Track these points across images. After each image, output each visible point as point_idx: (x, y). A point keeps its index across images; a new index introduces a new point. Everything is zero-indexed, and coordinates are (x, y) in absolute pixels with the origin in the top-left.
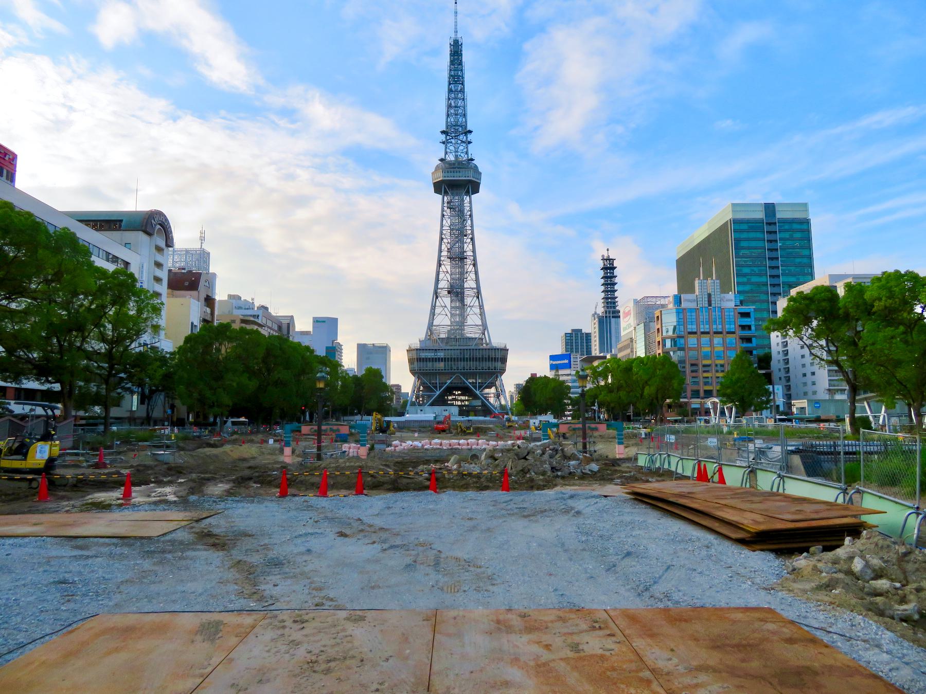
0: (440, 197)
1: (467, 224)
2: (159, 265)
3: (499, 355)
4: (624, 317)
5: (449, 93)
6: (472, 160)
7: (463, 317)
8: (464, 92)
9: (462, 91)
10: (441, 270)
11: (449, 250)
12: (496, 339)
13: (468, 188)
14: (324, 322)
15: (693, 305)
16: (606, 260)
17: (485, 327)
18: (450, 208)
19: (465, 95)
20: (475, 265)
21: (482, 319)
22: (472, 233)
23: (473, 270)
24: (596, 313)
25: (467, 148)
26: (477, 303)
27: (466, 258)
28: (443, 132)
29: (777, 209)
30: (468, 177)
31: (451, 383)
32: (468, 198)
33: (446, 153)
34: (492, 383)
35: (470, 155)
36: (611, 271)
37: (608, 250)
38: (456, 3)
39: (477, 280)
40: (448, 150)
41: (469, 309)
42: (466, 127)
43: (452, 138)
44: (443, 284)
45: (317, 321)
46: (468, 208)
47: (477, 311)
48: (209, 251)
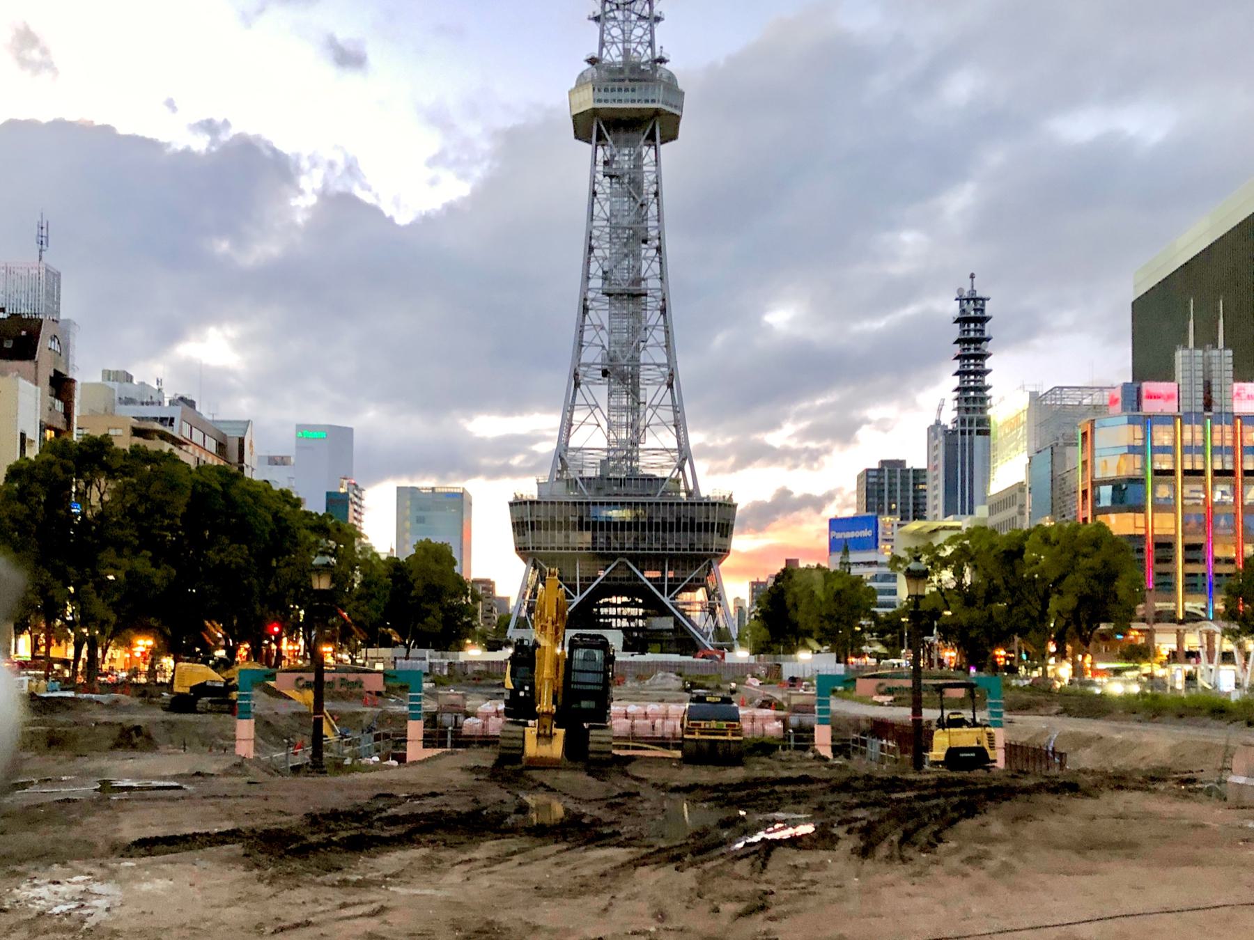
0: (587, 148)
1: (649, 215)
3: (715, 517)
10: (587, 321)
11: (606, 276)
16: (968, 300)
18: (611, 177)
20: (663, 311)
21: (678, 436)
23: (661, 322)
24: (938, 423)
25: (652, 32)
27: (646, 295)
30: (653, 101)
31: (607, 578)
32: (652, 151)
33: (602, 44)
34: (698, 580)
36: (979, 326)
37: (972, 276)
40: (607, 38)
41: (649, 412)
44: (592, 355)
46: (652, 177)
47: (668, 415)
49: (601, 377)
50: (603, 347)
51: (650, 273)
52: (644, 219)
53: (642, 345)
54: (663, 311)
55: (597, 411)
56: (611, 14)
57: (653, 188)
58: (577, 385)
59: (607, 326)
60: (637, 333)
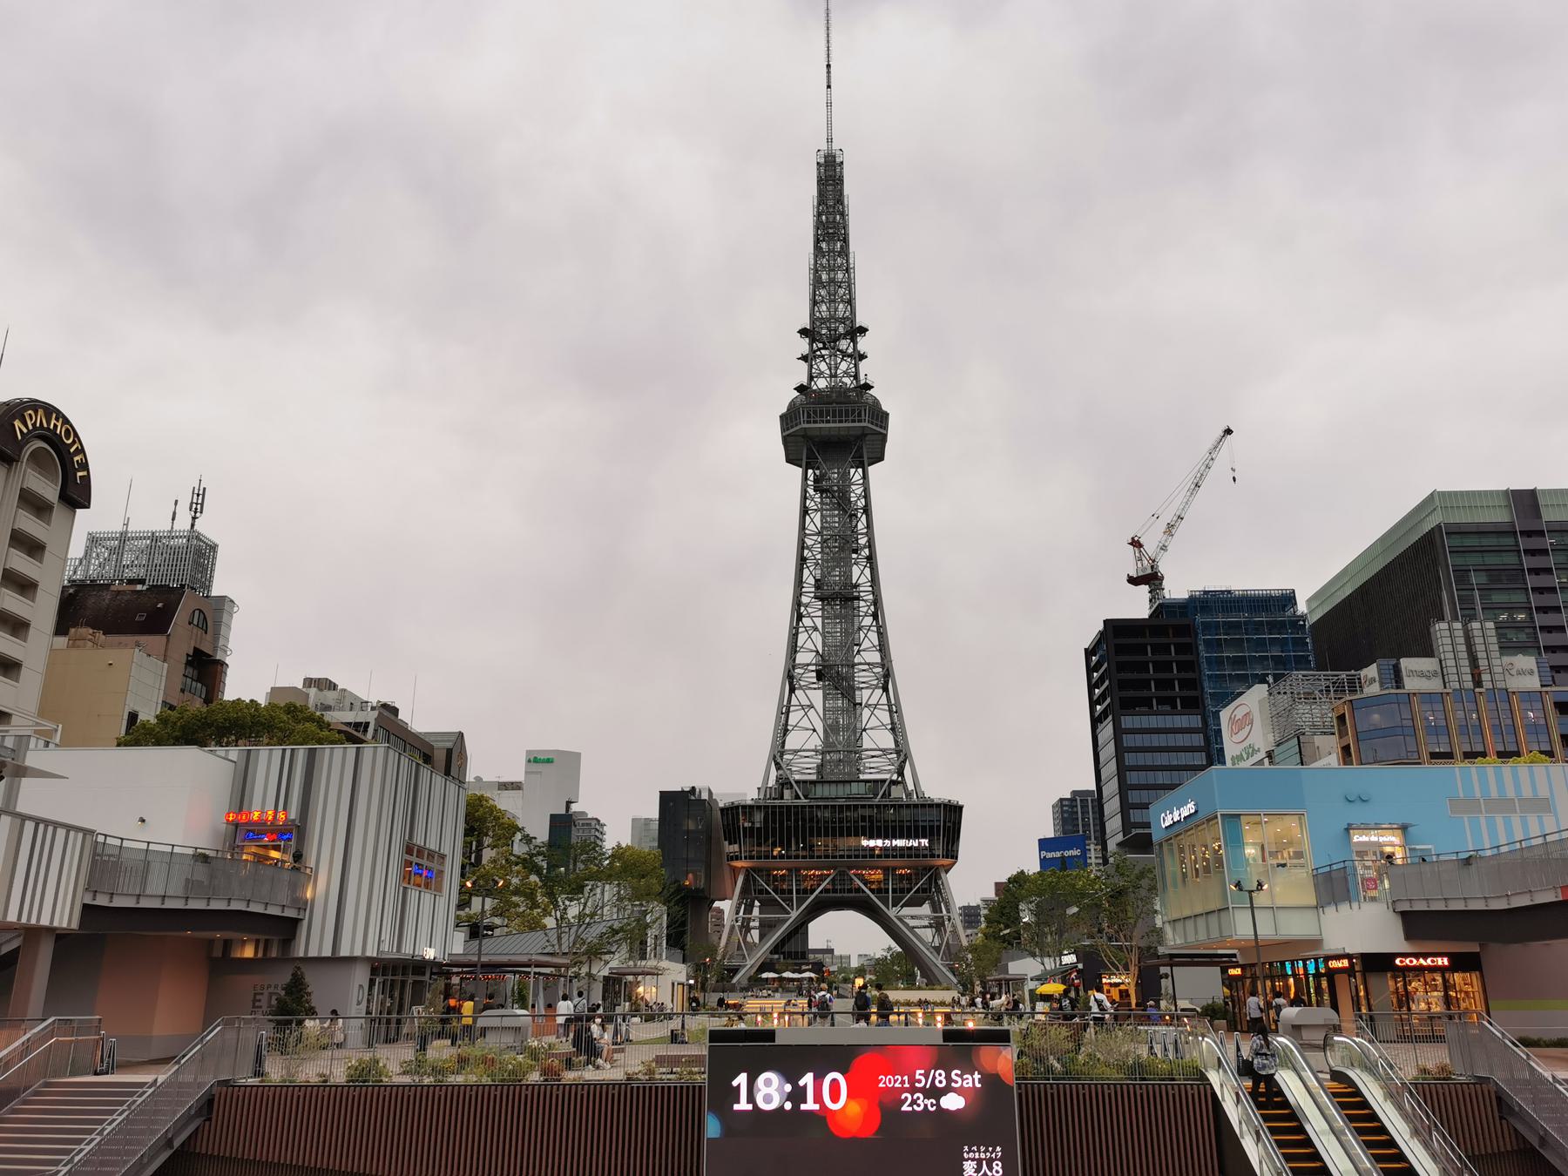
0: (798, 471)
2: (34, 548)
4: (1234, 733)
5: (816, 256)
6: (868, 387)
7: (856, 733)
8: (847, 256)
9: (845, 252)
11: (818, 584)
13: (860, 448)
14: (549, 761)
15: (1435, 685)
17: (902, 754)
19: (851, 261)
22: (871, 545)
25: (856, 366)
26: (884, 700)
29: (1541, 502)
30: (860, 421)
32: (860, 470)
33: (811, 378)
34: (924, 891)
35: (862, 377)
38: (829, 87)
39: (883, 647)
41: (866, 713)
42: (853, 321)
43: (824, 348)
45: (536, 761)
47: (885, 717)
48: (217, 542)
49: (815, 680)
50: (817, 652)
52: (854, 530)
53: (856, 648)
54: (875, 616)
55: (812, 713)
56: (818, 353)
58: (792, 690)
59: (820, 628)
60: (850, 643)
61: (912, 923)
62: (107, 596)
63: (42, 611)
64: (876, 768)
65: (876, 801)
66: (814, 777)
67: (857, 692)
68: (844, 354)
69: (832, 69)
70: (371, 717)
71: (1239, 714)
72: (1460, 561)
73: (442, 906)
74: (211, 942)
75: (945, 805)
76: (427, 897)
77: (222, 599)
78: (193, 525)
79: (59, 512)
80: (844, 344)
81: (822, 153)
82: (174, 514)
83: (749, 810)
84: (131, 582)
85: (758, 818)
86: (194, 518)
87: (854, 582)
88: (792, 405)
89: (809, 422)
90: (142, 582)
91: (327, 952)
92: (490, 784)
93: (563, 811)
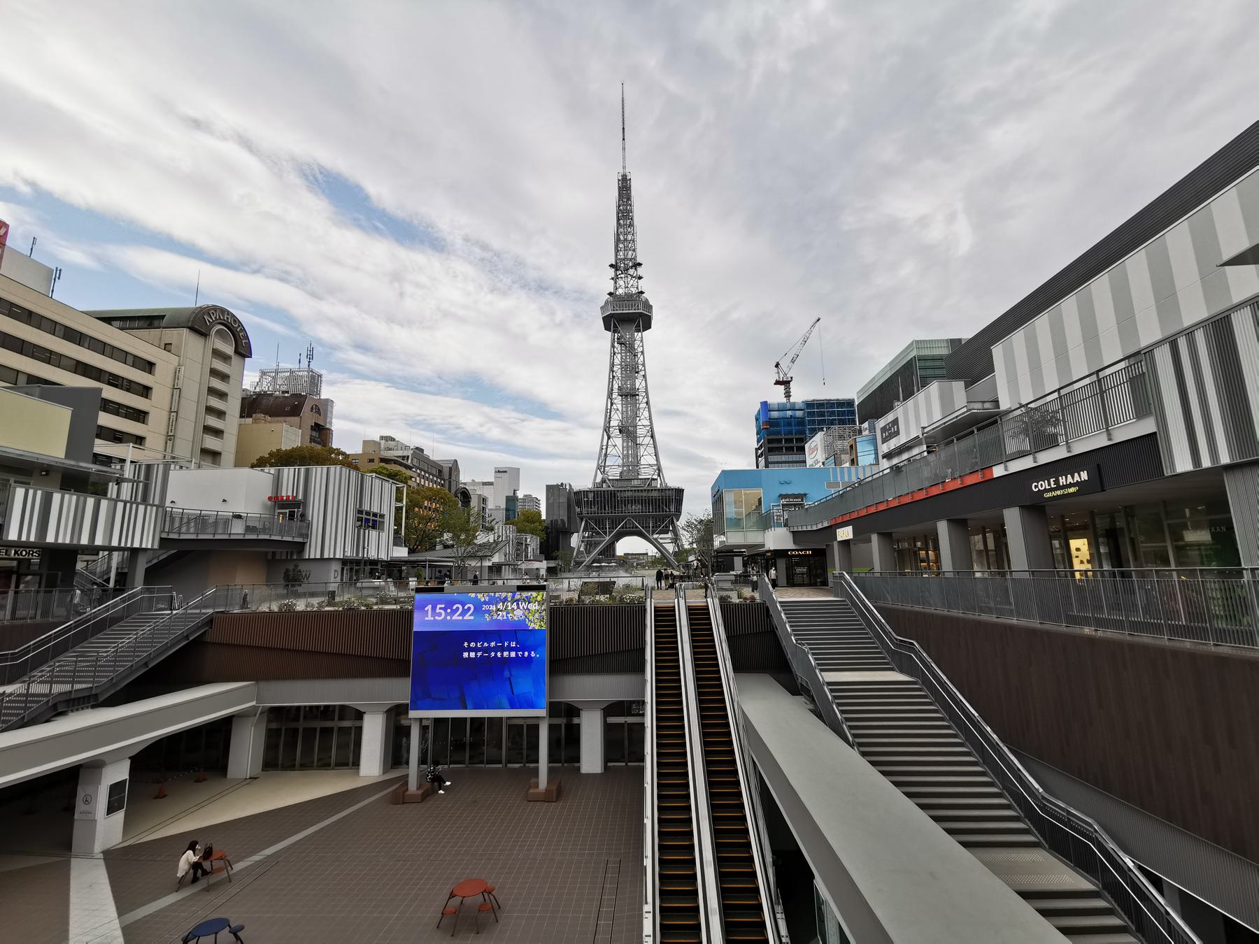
0: (609, 334)
6: (642, 293)
7: (637, 458)
9: (631, 225)
12: (672, 478)
13: (639, 321)
18: (621, 344)
20: (647, 403)
26: (652, 442)
27: (638, 395)
28: (611, 266)
30: (638, 309)
35: (640, 288)
38: (624, 139)
42: (635, 259)
43: (622, 273)
45: (499, 472)
51: (641, 387)
53: (638, 419)
57: (640, 349)
58: (609, 438)
61: (661, 541)
62: (272, 399)
63: (232, 407)
64: (646, 473)
65: (645, 488)
66: (618, 478)
67: (638, 439)
68: (632, 277)
69: (625, 131)
70: (410, 453)
71: (813, 446)
72: (923, 373)
73: (384, 536)
74: (267, 553)
75: (676, 489)
76: (374, 533)
77: (327, 400)
78: (309, 366)
79: (236, 360)
80: (631, 271)
81: (620, 174)
82: (300, 360)
83: (586, 493)
84: (283, 392)
85: (591, 496)
86: (309, 362)
87: (637, 387)
88: (607, 303)
89: (614, 310)
90: (287, 392)
91: (318, 556)
92: (479, 483)
93: (512, 495)
